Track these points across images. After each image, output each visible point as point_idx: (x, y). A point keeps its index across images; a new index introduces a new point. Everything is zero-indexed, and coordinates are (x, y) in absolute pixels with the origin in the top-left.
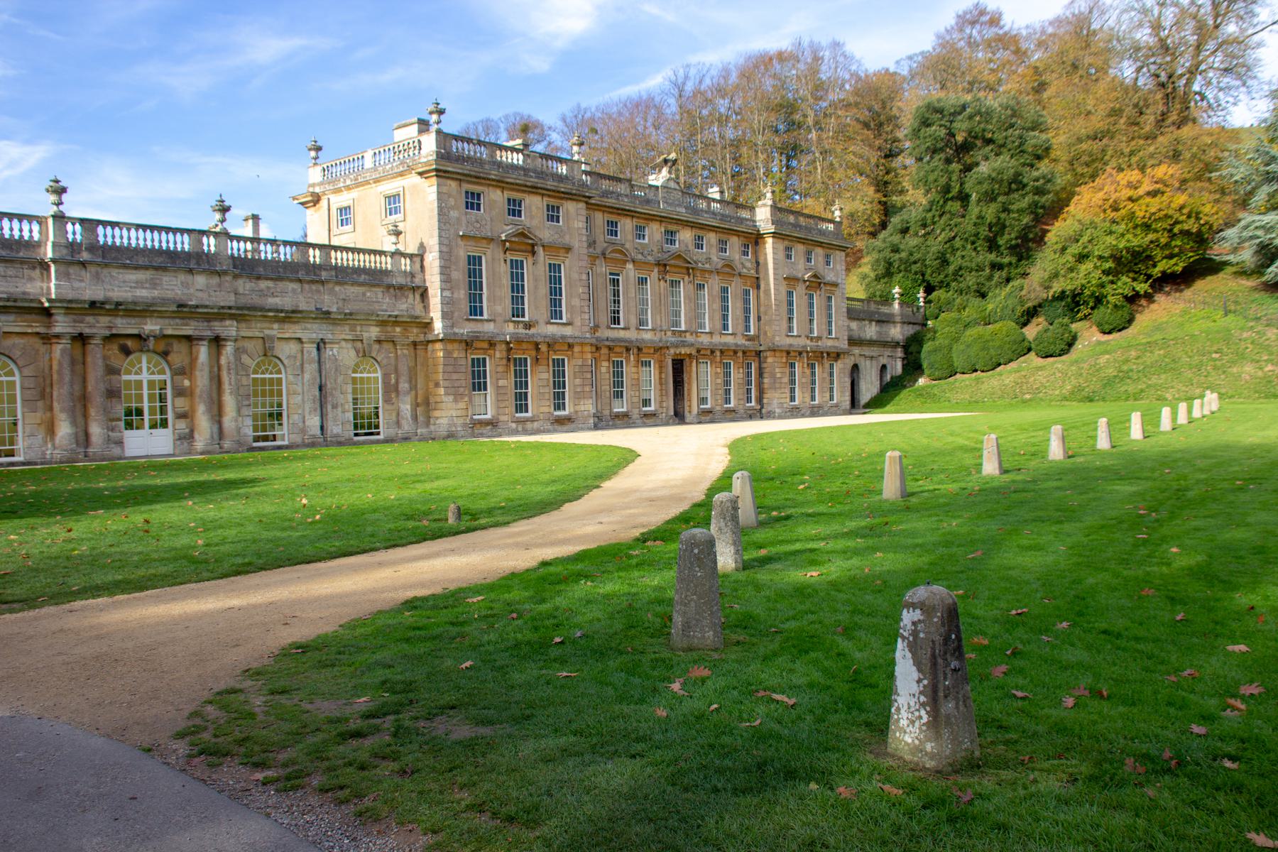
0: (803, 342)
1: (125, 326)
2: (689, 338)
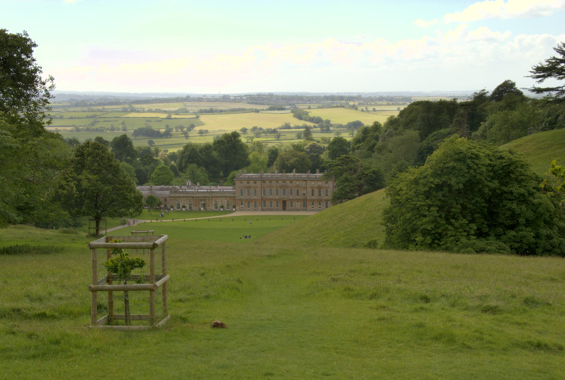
0: (316, 198)
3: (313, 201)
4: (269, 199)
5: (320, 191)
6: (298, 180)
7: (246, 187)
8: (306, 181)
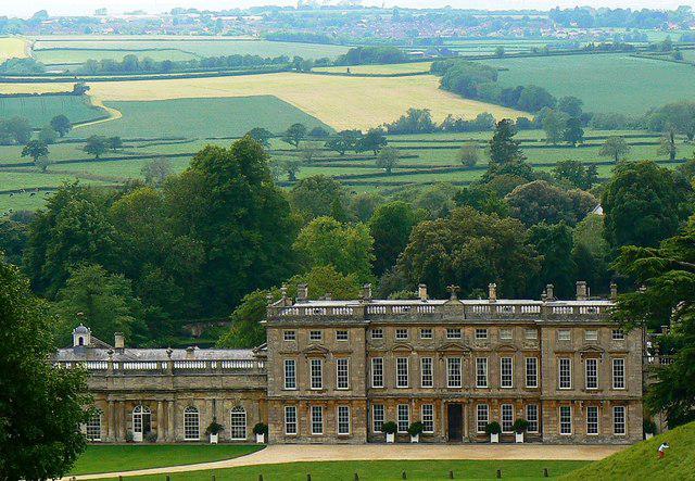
0: (577, 393)
1: (129, 397)
2: (463, 392)
3: (564, 406)
4: (397, 399)
5: (591, 369)
6: (508, 326)
7: (309, 354)
8: (538, 327)
